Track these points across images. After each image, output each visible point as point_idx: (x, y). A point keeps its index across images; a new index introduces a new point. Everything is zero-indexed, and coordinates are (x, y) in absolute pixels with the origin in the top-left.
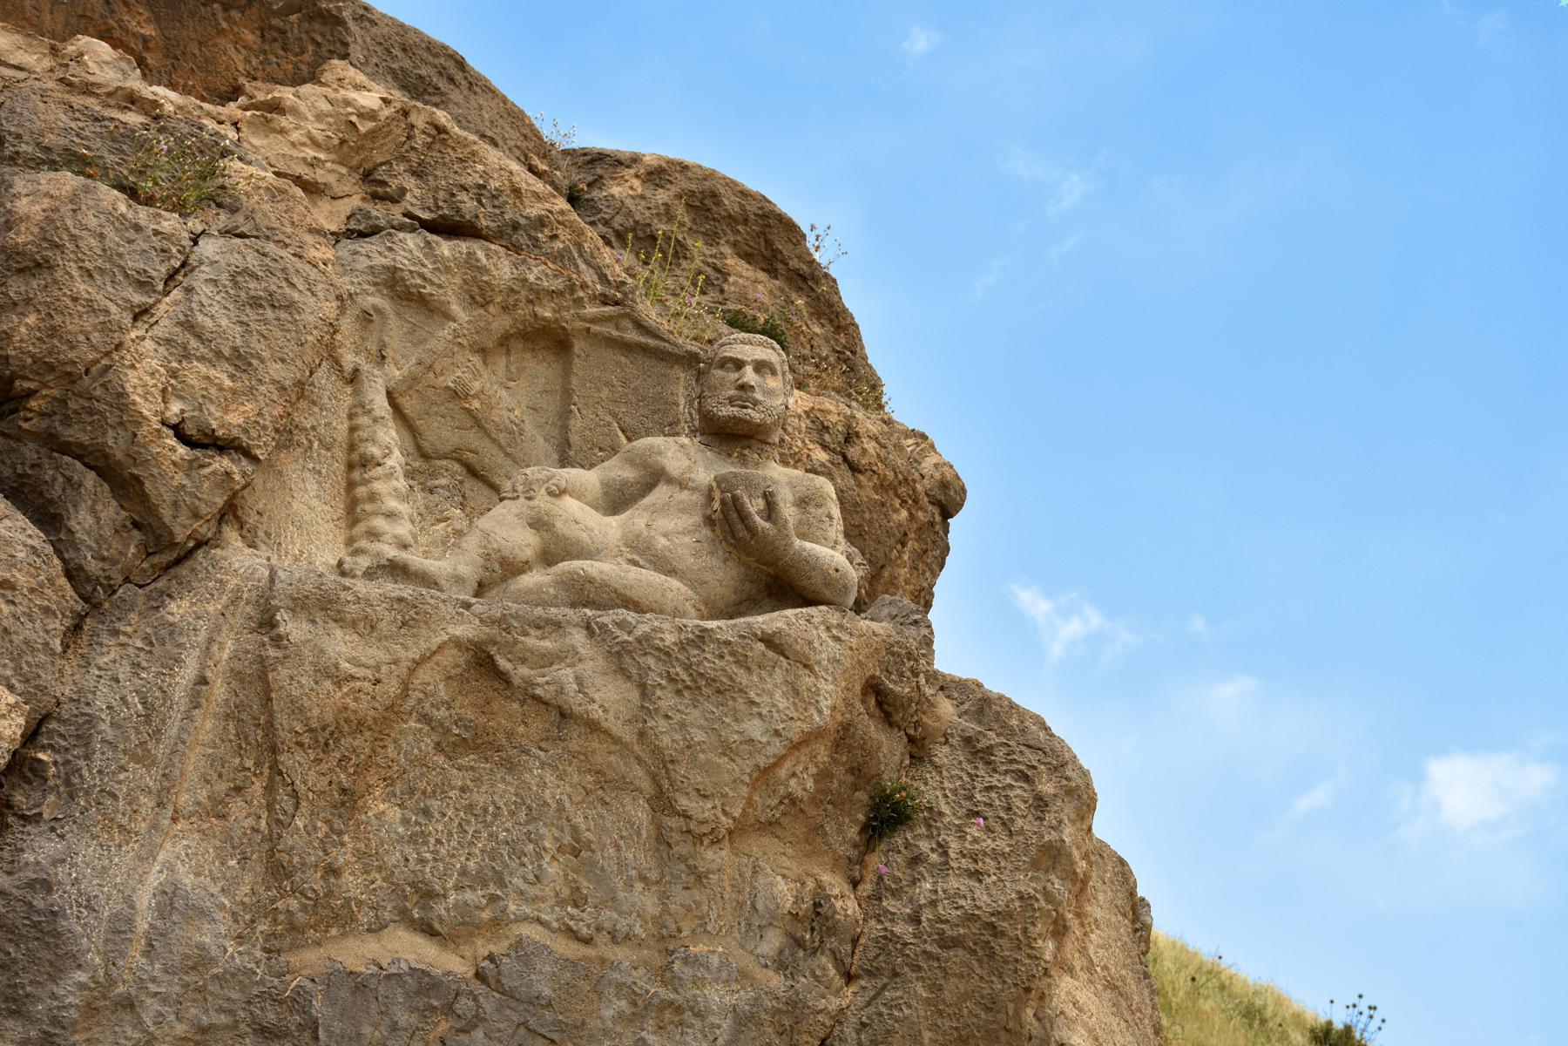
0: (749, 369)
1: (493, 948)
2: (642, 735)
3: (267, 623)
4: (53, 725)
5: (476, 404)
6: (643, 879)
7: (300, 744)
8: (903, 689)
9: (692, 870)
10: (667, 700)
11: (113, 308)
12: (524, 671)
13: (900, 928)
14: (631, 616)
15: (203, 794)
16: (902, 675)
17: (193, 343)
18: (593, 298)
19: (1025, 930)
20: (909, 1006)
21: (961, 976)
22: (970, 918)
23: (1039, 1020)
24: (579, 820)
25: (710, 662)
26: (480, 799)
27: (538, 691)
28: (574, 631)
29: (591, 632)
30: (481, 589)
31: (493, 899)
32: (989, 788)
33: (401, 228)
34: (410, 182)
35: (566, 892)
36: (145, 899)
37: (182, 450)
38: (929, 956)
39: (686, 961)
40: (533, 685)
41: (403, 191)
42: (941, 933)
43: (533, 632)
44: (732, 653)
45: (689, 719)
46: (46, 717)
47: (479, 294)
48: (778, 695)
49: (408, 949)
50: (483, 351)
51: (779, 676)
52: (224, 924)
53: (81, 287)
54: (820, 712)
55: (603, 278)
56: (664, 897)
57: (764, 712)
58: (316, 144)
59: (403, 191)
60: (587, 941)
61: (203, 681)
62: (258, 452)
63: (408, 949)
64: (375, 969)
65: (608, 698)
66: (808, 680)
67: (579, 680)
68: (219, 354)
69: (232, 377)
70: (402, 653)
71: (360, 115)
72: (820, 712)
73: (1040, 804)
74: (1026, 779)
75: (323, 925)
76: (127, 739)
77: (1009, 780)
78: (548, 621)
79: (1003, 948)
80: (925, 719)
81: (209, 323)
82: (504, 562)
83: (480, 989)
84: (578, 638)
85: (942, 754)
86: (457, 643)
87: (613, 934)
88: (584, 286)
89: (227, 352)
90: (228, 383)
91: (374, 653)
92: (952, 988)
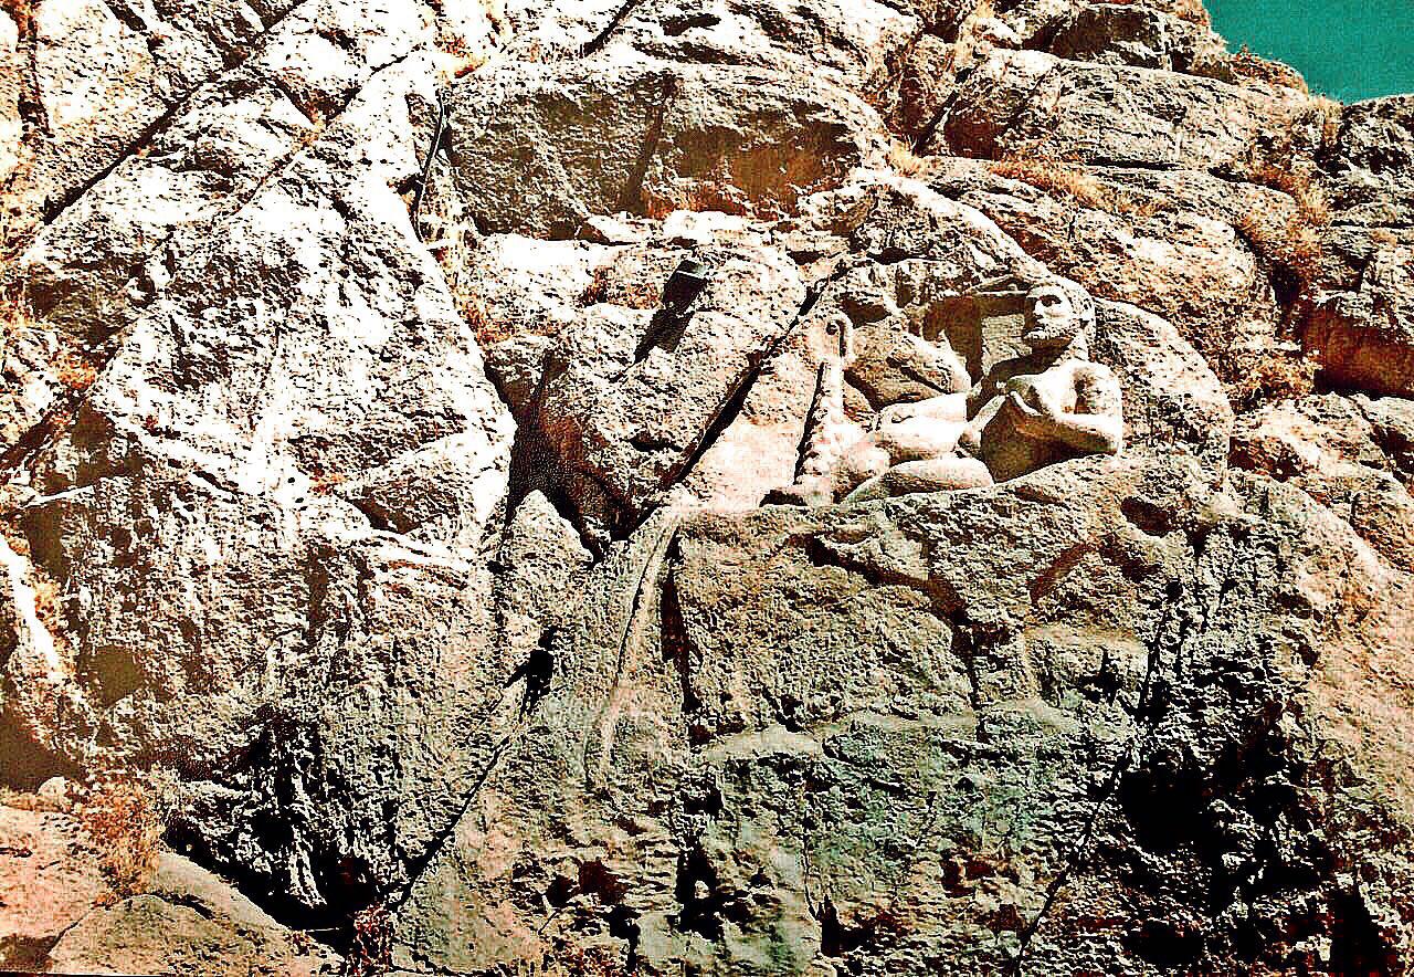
0: (1039, 303)
1: (837, 733)
2: (932, 574)
3: (673, 552)
4: (558, 633)
5: (910, 363)
6: (957, 669)
7: (698, 621)
8: (1162, 502)
9: (993, 659)
10: (945, 546)
11: (596, 380)
12: (846, 546)
13: (1169, 676)
14: (914, 496)
15: (648, 660)
16: (1160, 491)
17: (643, 387)
18: (988, 275)
19: (1265, 663)
20: (1177, 730)
21: (1216, 704)
22: (1216, 662)
23: (1300, 725)
24: (898, 641)
25: (975, 515)
26: (822, 635)
27: (856, 558)
28: (877, 514)
29: (888, 514)
30: (837, 498)
31: (834, 700)
32: (1241, 562)
33: (861, 265)
34: (875, 233)
35: (894, 687)
36: (608, 731)
37: (635, 454)
38: (1188, 692)
39: (993, 721)
40: (851, 555)
41: (869, 241)
42: (1195, 674)
43: (848, 521)
44: (995, 508)
45: (967, 557)
46: (554, 629)
47: (903, 295)
48: (1036, 528)
49: (779, 740)
50: (914, 329)
51: (1034, 516)
52: (663, 738)
53: (580, 371)
54: (1076, 534)
55: (997, 259)
56: (974, 682)
57: (1026, 541)
58: (817, 228)
59: (869, 241)
60: (913, 717)
61: (640, 591)
62: (679, 444)
63: (779, 740)
64: (753, 756)
65: (905, 556)
66: (1058, 515)
67: (882, 545)
68: (658, 391)
69: (666, 402)
70: (758, 552)
71: (845, 203)
72: (1076, 534)
73: (1281, 566)
74: (1275, 549)
75: (722, 730)
76: (596, 635)
77: (1260, 551)
78: (859, 512)
79: (1246, 679)
80: (1199, 517)
81: (654, 373)
82: (852, 475)
83: (824, 758)
84: (881, 517)
85: (1213, 541)
86: (795, 540)
87: (936, 711)
88: (979, 269)
89: (664, 388)
90: (662, 406)
91: (741, 554)
92: (1211, 715)
